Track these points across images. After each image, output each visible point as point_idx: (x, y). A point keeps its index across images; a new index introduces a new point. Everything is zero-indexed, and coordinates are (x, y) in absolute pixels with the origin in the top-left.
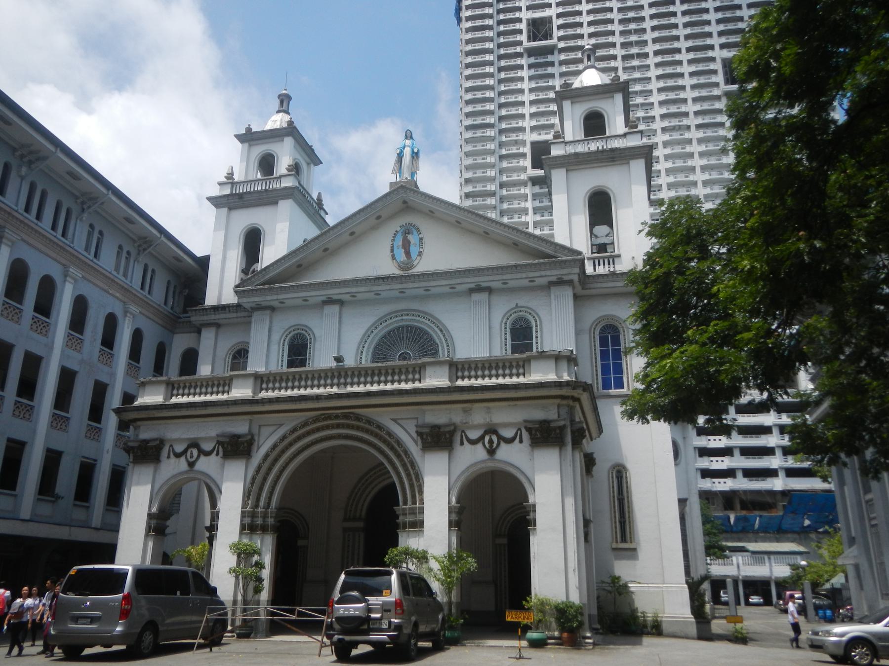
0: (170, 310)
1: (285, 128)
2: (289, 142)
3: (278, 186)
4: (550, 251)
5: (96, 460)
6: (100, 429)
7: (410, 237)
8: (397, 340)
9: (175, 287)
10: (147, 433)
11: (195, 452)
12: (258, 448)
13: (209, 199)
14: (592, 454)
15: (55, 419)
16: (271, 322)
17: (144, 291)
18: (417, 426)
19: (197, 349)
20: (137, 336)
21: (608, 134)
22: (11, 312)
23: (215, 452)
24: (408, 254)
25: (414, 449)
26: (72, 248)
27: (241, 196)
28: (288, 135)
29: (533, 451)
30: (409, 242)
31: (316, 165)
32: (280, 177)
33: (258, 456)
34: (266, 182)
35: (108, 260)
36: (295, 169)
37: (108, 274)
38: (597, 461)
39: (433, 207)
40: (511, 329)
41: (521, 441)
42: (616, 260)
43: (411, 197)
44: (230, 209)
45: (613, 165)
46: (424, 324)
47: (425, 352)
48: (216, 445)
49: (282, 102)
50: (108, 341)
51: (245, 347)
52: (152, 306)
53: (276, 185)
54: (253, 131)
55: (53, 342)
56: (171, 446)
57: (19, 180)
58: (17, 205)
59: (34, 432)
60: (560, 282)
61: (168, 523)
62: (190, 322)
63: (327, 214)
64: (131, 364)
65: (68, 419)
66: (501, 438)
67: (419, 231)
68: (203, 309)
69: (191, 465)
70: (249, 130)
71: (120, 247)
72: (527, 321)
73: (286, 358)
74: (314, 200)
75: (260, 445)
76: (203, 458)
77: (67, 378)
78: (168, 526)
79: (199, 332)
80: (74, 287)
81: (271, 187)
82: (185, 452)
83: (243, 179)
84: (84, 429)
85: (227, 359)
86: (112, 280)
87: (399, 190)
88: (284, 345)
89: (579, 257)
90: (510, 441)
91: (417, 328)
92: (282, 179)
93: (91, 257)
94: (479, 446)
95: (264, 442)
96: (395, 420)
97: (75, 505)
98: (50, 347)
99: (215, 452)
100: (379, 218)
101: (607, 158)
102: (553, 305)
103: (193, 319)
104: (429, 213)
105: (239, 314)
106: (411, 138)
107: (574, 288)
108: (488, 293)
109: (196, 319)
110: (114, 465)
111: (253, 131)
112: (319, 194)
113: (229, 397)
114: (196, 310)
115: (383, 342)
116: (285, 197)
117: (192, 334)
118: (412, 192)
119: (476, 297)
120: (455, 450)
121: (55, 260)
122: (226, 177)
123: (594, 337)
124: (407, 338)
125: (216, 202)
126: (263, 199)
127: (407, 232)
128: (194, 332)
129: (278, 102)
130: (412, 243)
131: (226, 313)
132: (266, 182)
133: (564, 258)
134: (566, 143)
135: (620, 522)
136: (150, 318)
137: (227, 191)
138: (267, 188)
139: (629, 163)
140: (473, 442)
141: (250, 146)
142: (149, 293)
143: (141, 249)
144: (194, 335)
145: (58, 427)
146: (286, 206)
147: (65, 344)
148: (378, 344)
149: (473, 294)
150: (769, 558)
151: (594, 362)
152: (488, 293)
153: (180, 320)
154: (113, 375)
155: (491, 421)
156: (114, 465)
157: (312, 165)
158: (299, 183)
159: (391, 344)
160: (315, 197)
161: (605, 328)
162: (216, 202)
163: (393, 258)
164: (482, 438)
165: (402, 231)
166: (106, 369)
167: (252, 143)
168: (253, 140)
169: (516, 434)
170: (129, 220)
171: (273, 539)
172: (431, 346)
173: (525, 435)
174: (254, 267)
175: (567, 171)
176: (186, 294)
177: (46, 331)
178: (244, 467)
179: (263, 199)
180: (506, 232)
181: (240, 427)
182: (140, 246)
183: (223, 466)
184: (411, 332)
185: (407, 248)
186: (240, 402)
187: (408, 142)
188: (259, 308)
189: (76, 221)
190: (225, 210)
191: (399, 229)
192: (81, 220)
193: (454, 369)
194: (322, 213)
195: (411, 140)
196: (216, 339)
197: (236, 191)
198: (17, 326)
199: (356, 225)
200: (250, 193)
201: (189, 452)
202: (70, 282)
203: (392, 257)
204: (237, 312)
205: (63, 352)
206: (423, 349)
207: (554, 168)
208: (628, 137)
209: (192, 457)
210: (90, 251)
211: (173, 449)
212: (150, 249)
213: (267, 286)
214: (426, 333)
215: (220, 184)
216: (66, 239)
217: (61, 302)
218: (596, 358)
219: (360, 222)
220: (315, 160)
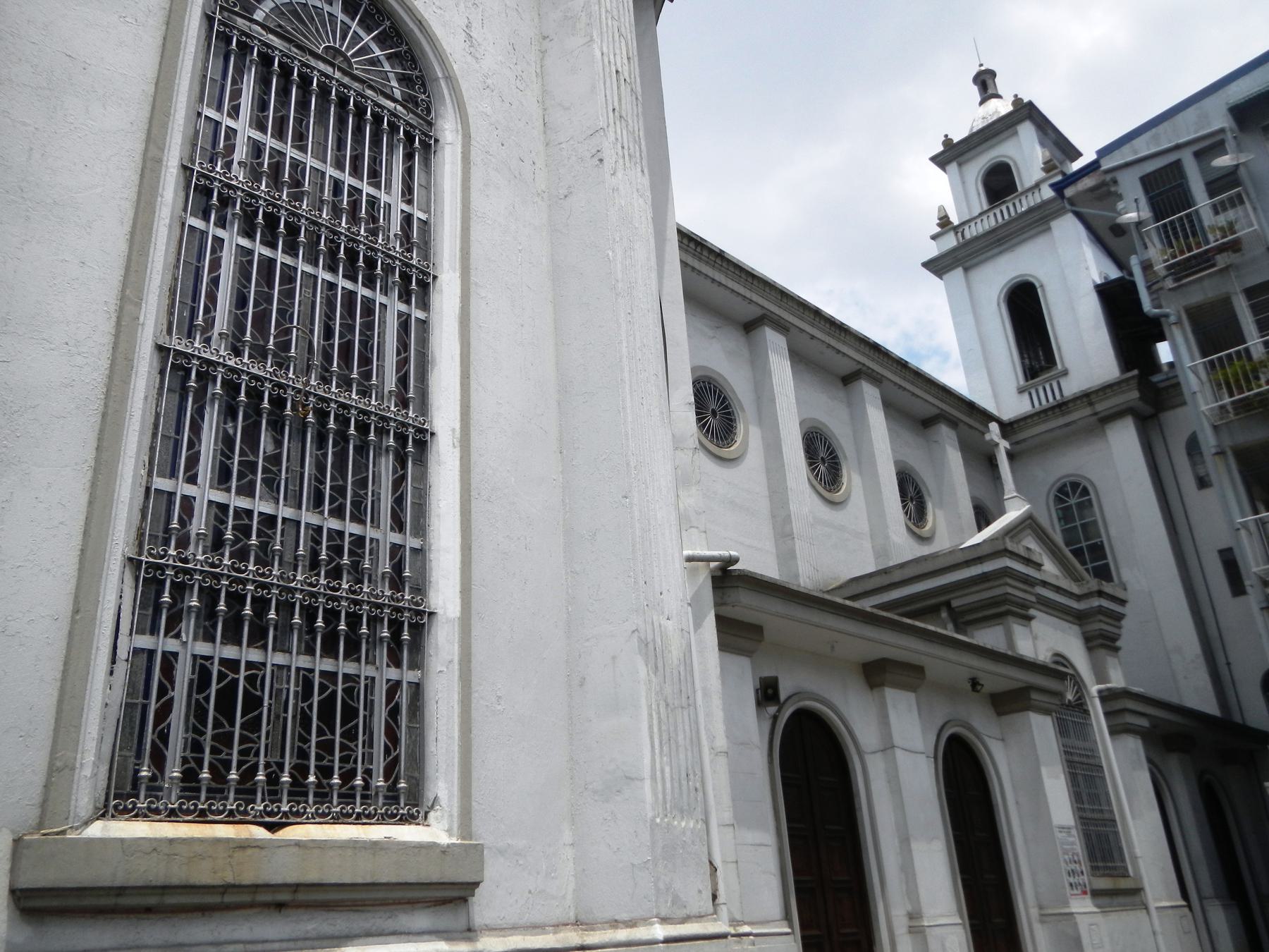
2: (1027, 131)
13: (925, 265)
28: (1020, 121)
70: (947, 142)
122: (939, 225)
125: (937, 266)
129: (975, 91)
137: (950, 241)
141: (960, 165)
157: (1068, 163)
162: (937, 266)
167: (961, 159)
168: (962, 154)
215: (934, 237)
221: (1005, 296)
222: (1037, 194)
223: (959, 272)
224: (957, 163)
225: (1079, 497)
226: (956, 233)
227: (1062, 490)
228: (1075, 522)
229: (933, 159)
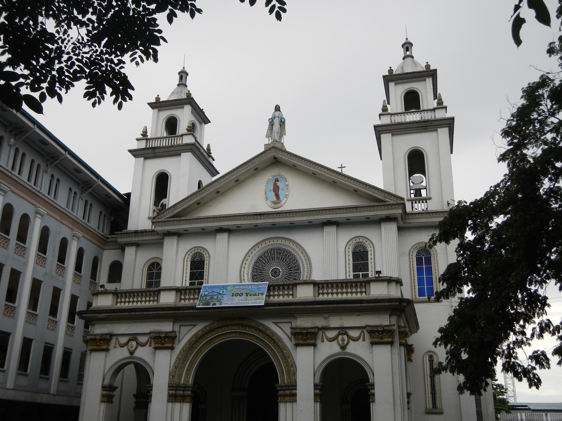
0: (101, 232)
1: (185, 99)
2: (188, 109)
3: (181, 143)
4: (381, 197)
5: (53, 345)
6: (56, 322)
7: (278, 184)
8: (270, 259)
9: (105, 216)
10: (99, 330)
11: (134, 343)
12: (179, 342)
13: (130, 151)
14: (412, 345)
15: (29, 316)
16: (178, 244)
17: (85, 220)
18: (291, 328)
19: (121, 261)
20: (80, 253)
21: (421, 109)
22: (20, 250)
24: (277, 196)
25: (289, 344)
26: (41, 193)
27: (153, 148)
28: (187, 104)
29: (372, 346)
30: (278, 187)
31: (206, 123)
32: (182, 135)
33: (179, 347)
34: (172, 139)
35: (62, 200)
36: (192, 129)
37: (63, 210)
38: (415, 350)
39: (296, 162)
40: (354, 254)
41: (364, 340)
42: (428, 201)
43: (280, 156)
44: (146, 158)
45: (426, 131)
46: (291, 247)
47: (291, 268)
48: (149, 338)
49: (181, 78)
50: (62, 259)
51: (158, 262)
52: (90, 231)
53: (179, 142)
54: (161, 100)
55: (28, 261)
56: (117, 339)
57: (8, 148)
58: (7, 166)
59: (15, 325)
60: (388, 219)
61: (115, 393)
62: (116, 241)
63: (214, 160)
64: (76, 274)
65: (37, 315)
66: (349, 337)
67: (286, 179)
68: (127, 233)
69: (132, 353)
70: (158, 99)
71: (70, 189)
72: (364, 247)
73: (189, 271)
74: (205, 151)
75: (180, 339)
76: (140, 348)
77: (36, 285)
78: (115, 395)
79: (123, 249)
80: (41, 221)
81: (175, 143)
82: (127, 344)
83: (154, 136)
84: (47, 323)
85: (144, 270)
86: (66, 214)
87: (271, 150)
88: (187, 262)
89: (402, 202)
90: (356, 340)
91: (284, 250)
92: (184, 137)
93: (52, 198)
94: (335, 343)
95: (184, 337)
96: (276, 323)
97: (40, 378)
98: (26, 264)
100: (256, 169)
101: (421, 127)
102: (383, 236)
103: (119, 240)
104: (293, 166)
105: (153, 238)
106: (279, 110)
107: (398, 223)
108: (336, 226)
109: (122, 240)
110: (65, 348)
111: (161, 100)
112: (209, 146)
113: (158, 305)
114: (122, 234)
115: (260, 261)
117: (117, 250)
118: (281, 152)
119: (327, 229)
120: (317, 345)
121: (30, 203)
122: (142, 135)
123: (412, 258)
124: (277, 257)
125: (135, 153)
126: (170, 151)
127: (277, 180)
128: (119, 249)
130: (280, 188)
131: (143, 236)
132: (172, 139)
133: (392, 202)
134: (391, 114)
135: (432, 393)
136: (88, 240)
137: (143, 145)
138: (173, 144)
139: (437, 130)
140: (331, 340)
141: (159, 111)
142: (88, 221)
143: (83, 190)
144: (118, 251)
145: (30, 322)
146: (187, 158)
147: (35, 262)
148: (256, 262)
149: (324, 227)
150: (546, 415)
151: (412, 276)
152: (336, 226)
153: (108, 240)
154: (64, 282)
155: (343, 325)
156: (65, 348)
157: (203, 124)
158: (196, 140)
159: (266, 262)
160: (205, 147)
161: (420, 252)
162: (135, 153)
163: (267, 199)
164: (336, 338)
165: (273, 179)
166: (60, 278)
169: (361, 334)
170: (78, 171)
171: (190, 406)
172: (295, 264)
173: (367, 335)
174: (164, 201)
175: (392, 135)
176: (112, 220)
177: (24, 254)
178: (169, 355)
179: (170, 151)
180: (348, 182)
181: (167, 327)
182: (82, 188)
183: (154, 353)
184: (280, 253)
185: (277, 192)
186: (167, 309)
187: (277, 113)
188: (169, 234)
189: (43, 173)
190: (142, 159)
191: (271, 178)
192: (46, 172)
193: (317, 288)
194: (210, 160)
195: (279, 112)
196: (136, 254)
197: (149, 146)
198: (5, 250)
199: (240, 175)
200: (159, 148)
201: (130, 343)
202: (39, 218)
203: (266, 198)
204: (152, 236)
205: (34, 268)
206: (289, 266)
207: (383, 133)
208: (437, 111)
209: (132, 347)
210: (51, 195)
211: (119, 341)
212: (90, 190)
213: (175, 219)
214: (290, 254)
215: (137, 140)
216: (37, 187)
217: (32, 232)
218: (414, 274)
219: (243, 173)
220: (206, 121)
221: (156, 176)
222: (181, 139)
223: (142, 159)
224: (158, 109)
225: (157, 270)
226: (147, 142)
227: (152, 265)
228: (153, 280)
229: (150, 104)
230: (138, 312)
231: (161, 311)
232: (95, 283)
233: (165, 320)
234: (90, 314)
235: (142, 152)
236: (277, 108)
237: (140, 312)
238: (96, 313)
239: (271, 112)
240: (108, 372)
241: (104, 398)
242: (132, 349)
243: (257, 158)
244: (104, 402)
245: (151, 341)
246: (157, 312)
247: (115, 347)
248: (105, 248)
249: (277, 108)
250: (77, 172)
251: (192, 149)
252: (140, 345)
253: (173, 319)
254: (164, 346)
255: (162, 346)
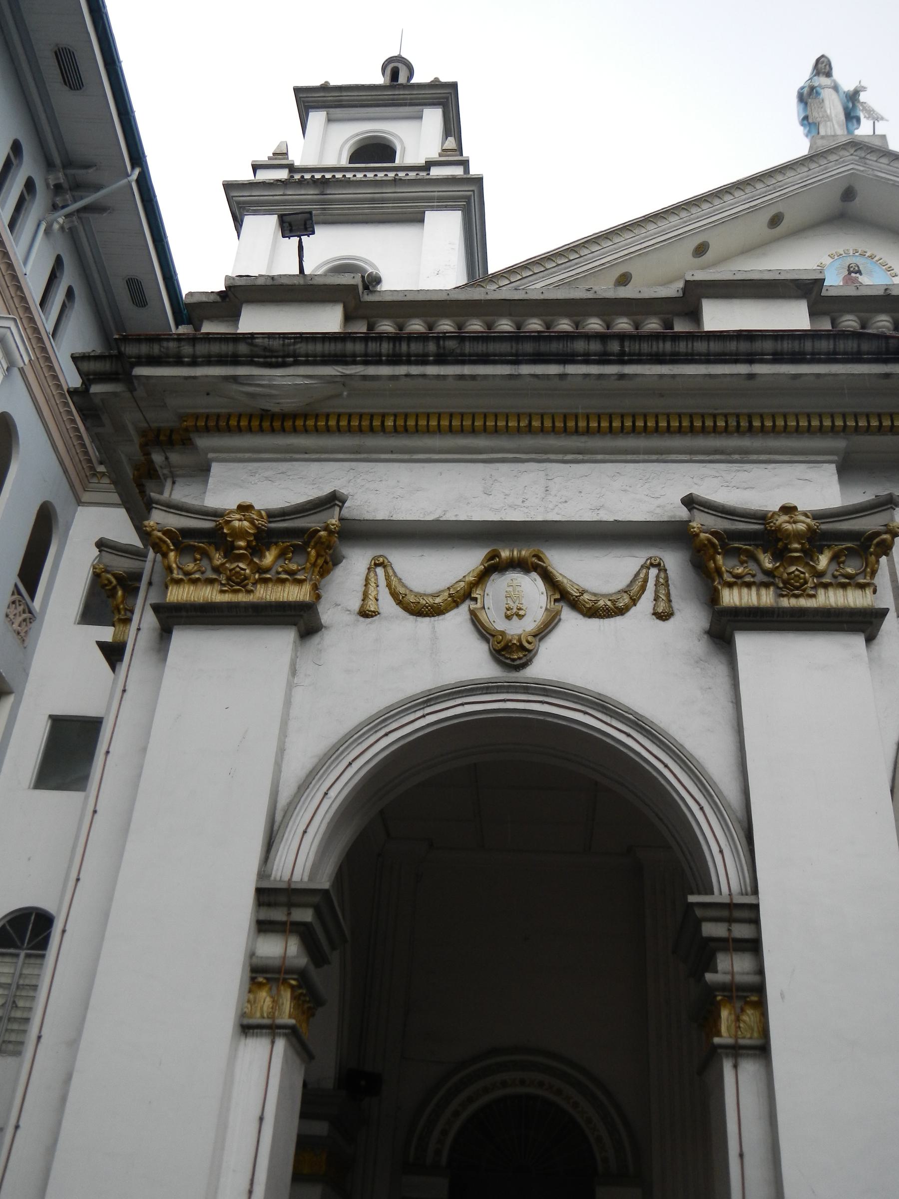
23: (646, 602)
48: (647, 566)
67: (890, 269)
99: (646, 602)
106: (829, 74)
116: (444, 204)
118: (884, 160)
126: (383, 201)
141: (330, 120)
167: (338, 112)
168: (339, 105)
199: (723, 222)
219: (735, 217)
224: (327, 114)
230: (587, 359)
231: (778, 358)
232: (30, 612)
233: (773, 443)
234: (194, 363)
235: (277, 194)
236: (823, 67)
237: (604, 359)
238: (250, 361)
239: (802, 75)
240: (304, 786)
241: (264, 998)
242: (515, 629)
243: (790, 173)
244: (271, 1029)
245: (664, 583)
246: (742, 369)
247: (365, 614)
248: (86, 497)
249: (823, 67)
250: (66, 81)
251: (468, 199)
252: (575, 604)
253: (840, 444)
254: (803, 602)
255: (785, 603)
